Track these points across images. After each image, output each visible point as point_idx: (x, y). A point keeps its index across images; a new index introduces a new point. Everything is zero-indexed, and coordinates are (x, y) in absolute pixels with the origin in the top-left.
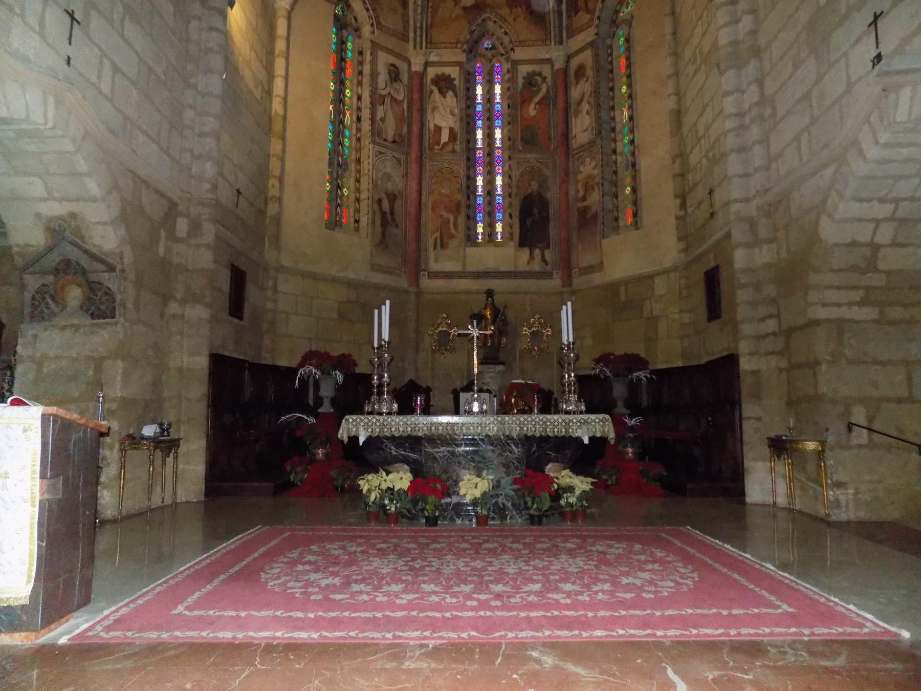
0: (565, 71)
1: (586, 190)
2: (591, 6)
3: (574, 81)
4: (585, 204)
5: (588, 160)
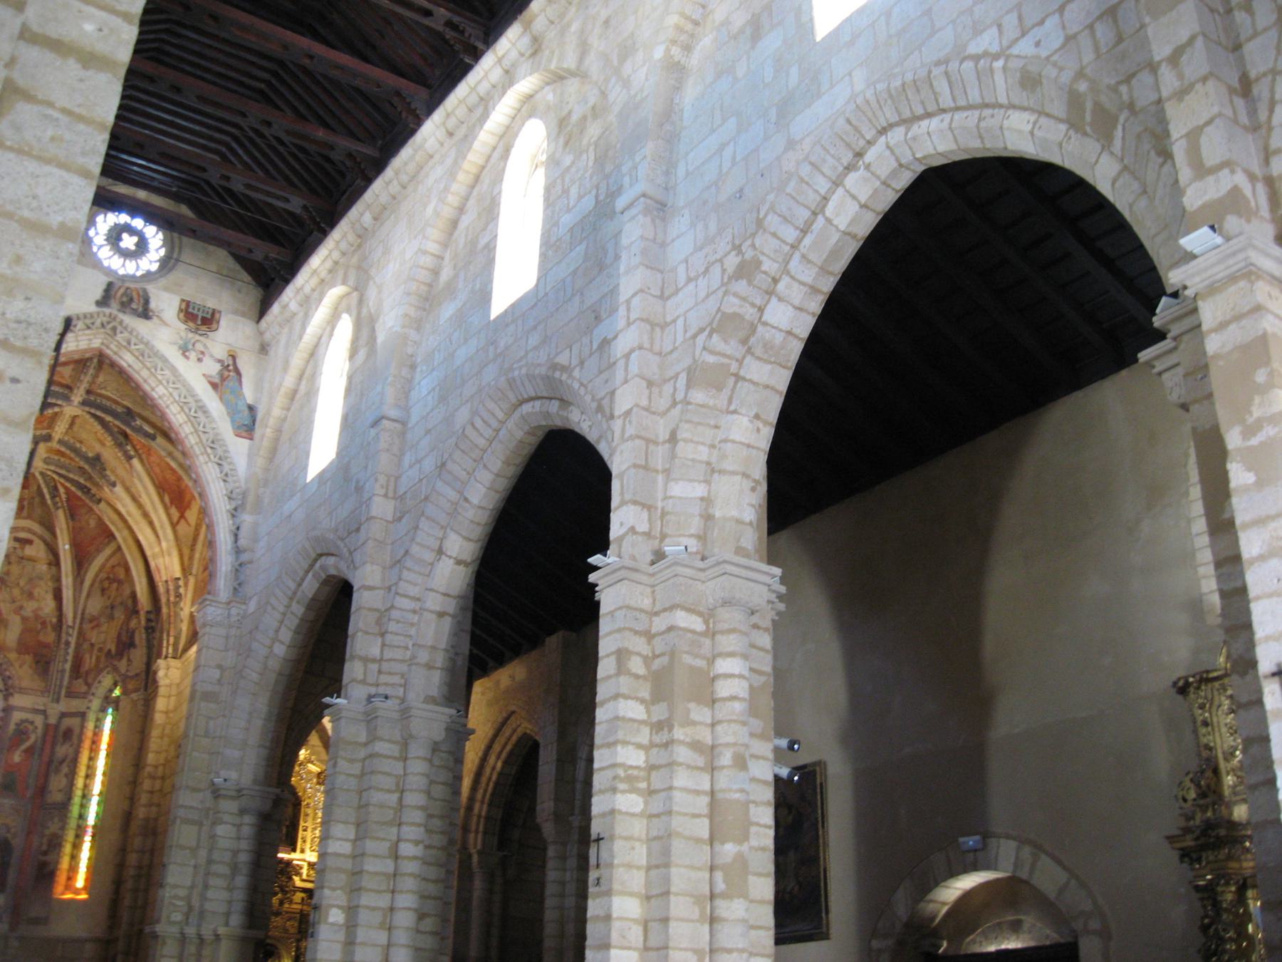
0: (57, 727)
1: (49, 845)
2: (90, 681)
3: (61, 739)
4: (43, 858)
5: (56, 820)
